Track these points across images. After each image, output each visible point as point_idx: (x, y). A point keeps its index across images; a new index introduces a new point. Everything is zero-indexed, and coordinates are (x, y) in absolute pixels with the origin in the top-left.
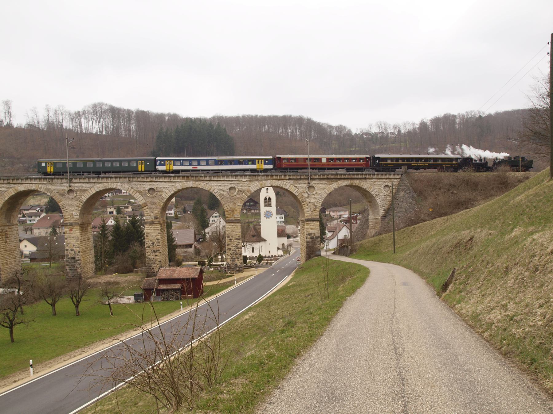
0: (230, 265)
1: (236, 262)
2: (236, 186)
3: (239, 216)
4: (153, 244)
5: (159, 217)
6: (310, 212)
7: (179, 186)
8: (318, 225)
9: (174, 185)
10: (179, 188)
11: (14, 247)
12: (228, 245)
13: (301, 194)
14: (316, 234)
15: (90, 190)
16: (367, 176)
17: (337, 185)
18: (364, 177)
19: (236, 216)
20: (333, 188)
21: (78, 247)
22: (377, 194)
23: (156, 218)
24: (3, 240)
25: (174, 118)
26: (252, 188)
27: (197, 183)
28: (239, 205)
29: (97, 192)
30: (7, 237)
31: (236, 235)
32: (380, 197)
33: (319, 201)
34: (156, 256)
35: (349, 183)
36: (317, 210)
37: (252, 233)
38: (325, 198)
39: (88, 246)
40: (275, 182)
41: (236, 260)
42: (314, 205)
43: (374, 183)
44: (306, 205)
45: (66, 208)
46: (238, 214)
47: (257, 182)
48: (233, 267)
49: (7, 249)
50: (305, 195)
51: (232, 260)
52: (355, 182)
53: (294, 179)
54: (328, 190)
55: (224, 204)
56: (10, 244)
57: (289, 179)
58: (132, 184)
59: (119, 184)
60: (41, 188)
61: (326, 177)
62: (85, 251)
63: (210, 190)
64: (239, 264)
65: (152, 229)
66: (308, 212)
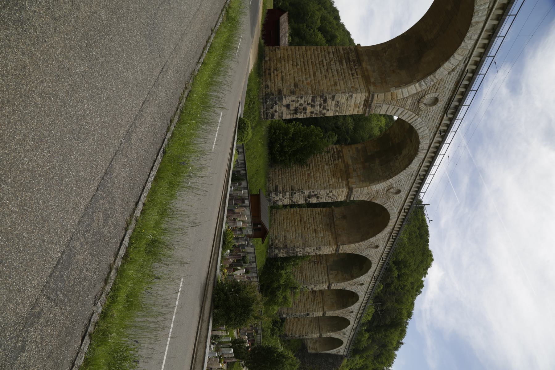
11: (305, 274)
30: (315, 264)
39: (306, 229)
56: (308, 269)
62: (301, 221)
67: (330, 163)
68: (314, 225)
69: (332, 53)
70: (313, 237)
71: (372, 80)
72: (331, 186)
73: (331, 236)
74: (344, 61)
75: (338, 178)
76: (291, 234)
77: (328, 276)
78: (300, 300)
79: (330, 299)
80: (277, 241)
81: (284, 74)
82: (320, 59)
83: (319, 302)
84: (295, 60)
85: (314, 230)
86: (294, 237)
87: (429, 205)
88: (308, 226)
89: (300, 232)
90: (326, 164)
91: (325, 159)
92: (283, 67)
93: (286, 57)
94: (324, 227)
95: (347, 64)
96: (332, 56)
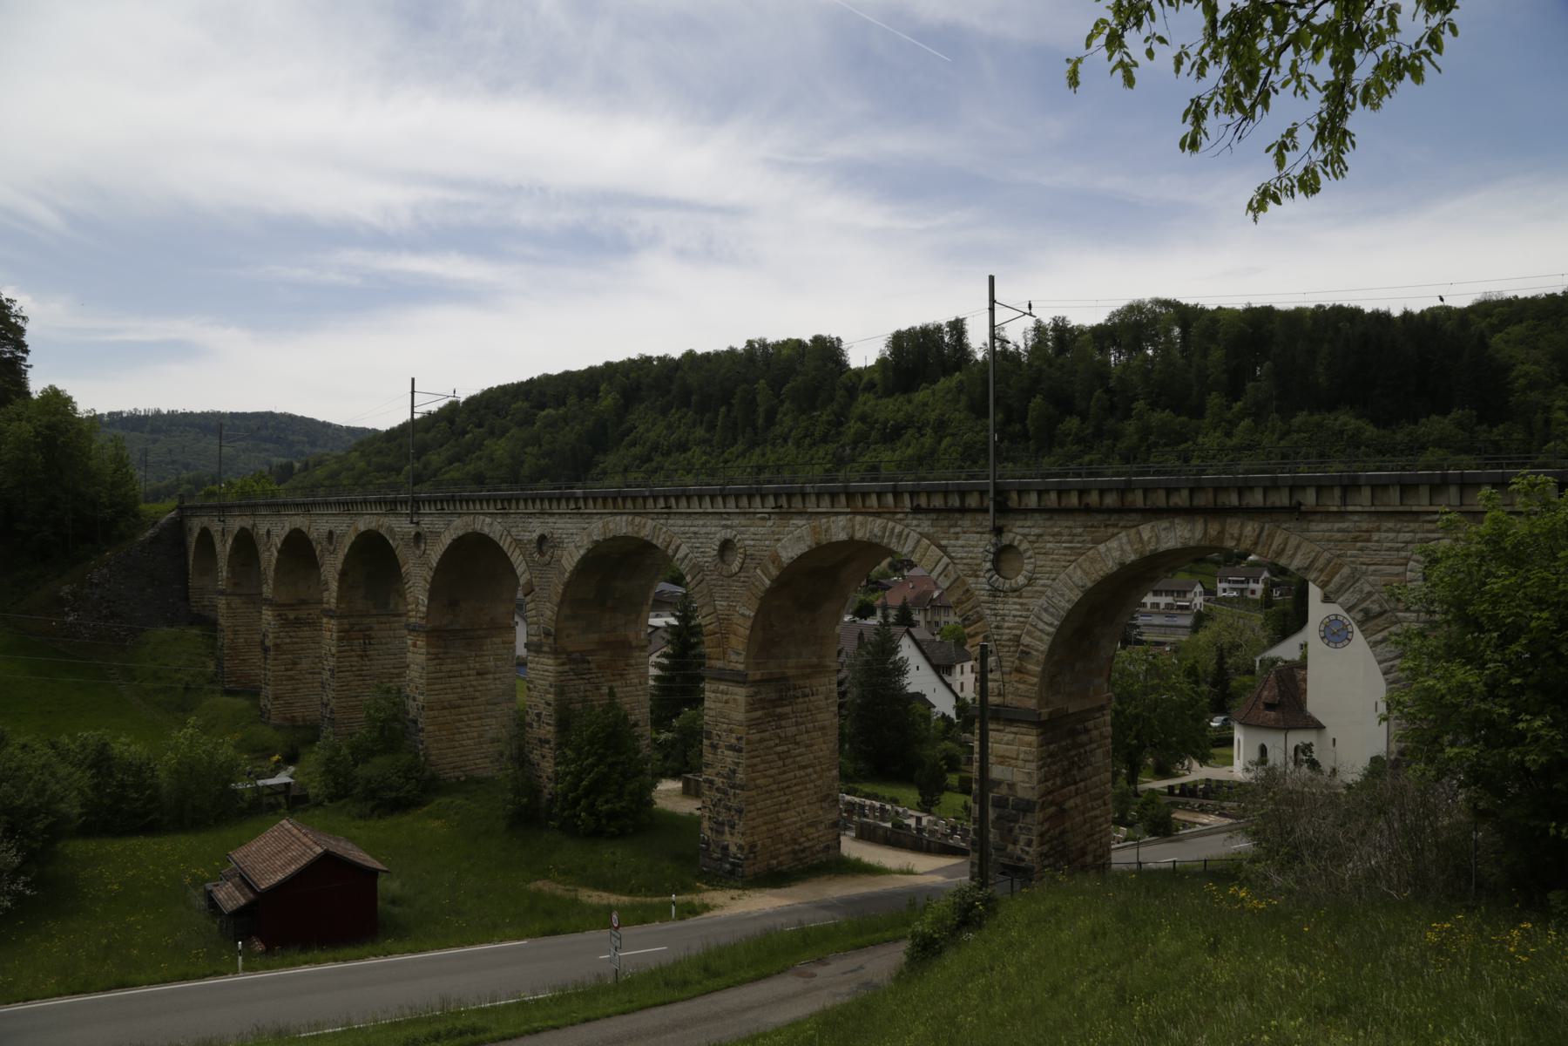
0: (708, 844)
1: (724, 838)
2: (738, 537)
3: (741, 659)
4: (539, 715)
5: (553, 630)
7: (596, 531)
8: (1030, 745)
9: (586, 526)
10: (595, 538)
11: (395, 668)
12: (707, 765)
13: (964, 583)
17: (1130, 542)
18: (1282, 499)
19: (733, 657)
20: (1110, 564)
21: (423, 694)
22: (1376, 608)
23: (548, 634)
24: (352, 650)
26: (784, 547)
27: (638, 520)
28: (743, 615)
29: (454, 540)
30: (370, 644)
31: (731, 731)
33: (1041, 625)
34: (544, 757)
35: (1198, 534)
37: (1265, 693)
38: (1071, 612)
39: (478, 694)
40: (862, 525)
41: (727, 829)
43: (1355, 540)
46: (741, 647)
47: (804, 522)
48: (715, 856)
49: (364, 673)
50: (980, 586)
51: (715, 826)
52: (1236, 532)
54: (1087, 574)
57: (917, 510)
58: (511, 519)
59: (488, 520)
60: (381, 526)
62: (459, 707)
63: (669, 545)
64: (733, 849)
65: (539, 667)
67: (597, 681)
68: (469, 675)
69: (762, 735)
70: (495, 679)
71: (815, 660)
72: (643, 680)
73: (494, 639)
74: (779, 710)
76: (487, 728)
81: (804, 824)
82: (775, 757)
84: (777, 807)
85: (479, 677)
86: (494, 721)
87: (413, 380)
88: (468, 689)
89: (482, 707)
90: (598, 688)
91: (586, 691)
92: (790, 828)
93: (771, 826)
94: (473, 654)
95: (786, 705)
96: (767, 733)
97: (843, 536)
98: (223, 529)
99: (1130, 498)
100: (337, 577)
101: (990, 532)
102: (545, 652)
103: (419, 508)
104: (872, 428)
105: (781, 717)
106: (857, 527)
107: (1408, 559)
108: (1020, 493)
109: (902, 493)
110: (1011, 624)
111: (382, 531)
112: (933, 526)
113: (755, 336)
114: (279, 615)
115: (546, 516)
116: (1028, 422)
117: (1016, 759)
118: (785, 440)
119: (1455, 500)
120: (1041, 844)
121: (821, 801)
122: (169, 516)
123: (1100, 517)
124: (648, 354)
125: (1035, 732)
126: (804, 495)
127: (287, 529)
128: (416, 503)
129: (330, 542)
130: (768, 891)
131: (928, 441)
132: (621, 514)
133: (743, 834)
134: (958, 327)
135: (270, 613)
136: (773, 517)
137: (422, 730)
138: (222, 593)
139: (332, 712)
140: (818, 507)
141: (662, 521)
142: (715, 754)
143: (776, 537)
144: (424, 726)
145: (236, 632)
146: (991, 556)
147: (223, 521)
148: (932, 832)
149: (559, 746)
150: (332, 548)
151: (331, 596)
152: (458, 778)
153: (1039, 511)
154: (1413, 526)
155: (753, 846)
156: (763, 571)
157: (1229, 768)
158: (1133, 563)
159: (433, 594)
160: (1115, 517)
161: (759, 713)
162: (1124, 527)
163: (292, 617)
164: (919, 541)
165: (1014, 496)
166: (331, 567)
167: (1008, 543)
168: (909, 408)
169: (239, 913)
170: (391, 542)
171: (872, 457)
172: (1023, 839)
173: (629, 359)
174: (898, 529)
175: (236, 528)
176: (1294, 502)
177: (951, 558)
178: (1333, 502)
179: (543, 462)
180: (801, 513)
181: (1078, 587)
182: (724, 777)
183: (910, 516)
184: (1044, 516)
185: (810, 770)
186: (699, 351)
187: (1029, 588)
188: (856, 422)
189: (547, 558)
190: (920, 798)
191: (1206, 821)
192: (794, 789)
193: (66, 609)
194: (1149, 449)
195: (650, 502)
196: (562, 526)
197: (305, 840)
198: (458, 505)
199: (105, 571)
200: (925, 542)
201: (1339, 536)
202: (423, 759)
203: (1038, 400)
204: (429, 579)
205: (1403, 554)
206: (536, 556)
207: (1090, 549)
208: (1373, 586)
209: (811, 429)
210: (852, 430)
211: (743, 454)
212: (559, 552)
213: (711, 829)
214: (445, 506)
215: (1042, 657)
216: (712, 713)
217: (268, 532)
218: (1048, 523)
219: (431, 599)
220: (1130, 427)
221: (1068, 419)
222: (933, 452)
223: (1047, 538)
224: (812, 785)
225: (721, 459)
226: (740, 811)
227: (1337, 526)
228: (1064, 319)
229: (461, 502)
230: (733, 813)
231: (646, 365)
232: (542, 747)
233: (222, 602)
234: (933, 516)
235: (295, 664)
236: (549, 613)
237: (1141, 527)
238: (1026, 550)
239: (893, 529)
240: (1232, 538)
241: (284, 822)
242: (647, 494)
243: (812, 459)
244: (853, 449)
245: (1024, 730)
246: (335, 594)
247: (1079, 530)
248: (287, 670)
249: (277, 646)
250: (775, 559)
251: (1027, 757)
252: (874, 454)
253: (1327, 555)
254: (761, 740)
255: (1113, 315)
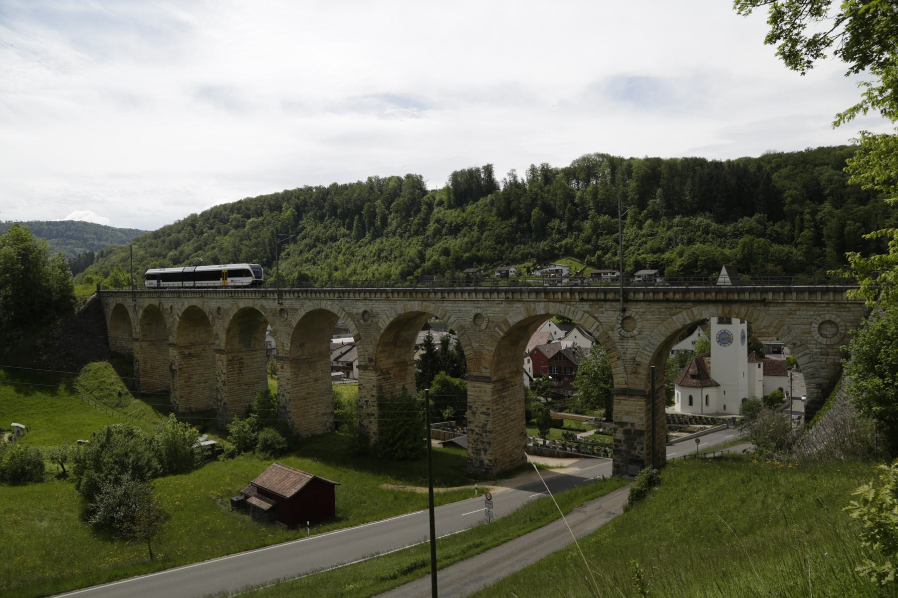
0: (472, 460)
1: (481, 457)
3: (488, 371)
4: (367, 401)
5: (374, 359)
6: (625, 375)
8: (641, 406)
10: (400, 312)
12: (470, 422)
13: (607, 334)
14: (636, 425)
15: (299, 311)
16: (770, 296)
18: (758, 296)
19: (483, 370)
21: (289, 393)
22: (799, 343)
24: (234, 371)
25: (694, 166)
26: (510, 317)
27: (425, 303)
28: (488, 350)
30: (243, 367)
31: (483, 405)
32: (807, 351)
33: (646, 352)
34: (370, 422)
36: (640, 371)
37: (691, 370)
39: (315, 391)
41: (482, 452)
42: (634, 359)
43: (789, 314)
44: (615, 359)
45: (278, 335)
48: (476, 466)
49: (240, 382)
50: (615, 335)
51: (475, 451)
53: (591, 300)
55: (465, 346)
57: (582, 300)
59: (329, 303)
61: (661, 296)
62: (305, 399)
64: (486, 462)
65: (366, 377)
66: (621, 375)
70: (323, 383)
71: (515, 369)
74: (503, 394)
75: (407, 374)
77: (256, 351)
78: (201, 376)
79: (200, 334)
80: (328, 424)
82: (502, 416)
83: (203, 350)
90: (394, 387)
93: (502, 450)
97: (543, 312)
98: (135, 305)
99: (687, 296)
100: (225, 332)
101: (619, 311)
102: (370, 370)
103: (282, 296)
104: (443, 226)
105: (504, 397)
106: (550, 308)
107: (812, 323)
108: (634, 293)
109: (574, 293)
110: (631, 352)
111: (258, 308)
112: (590, 308)
113: (372, 175)
114: (181, 352)
115: (367, 301)
116: (531, 221)
117: (635, 412)
118: (394, 234)
119: (831, 298)
120: (647, 449)
121: (520, 436)
122: (92, 297)
123: (673, 304)
124: (310, 186)
125: (644, 400)
126: (521, 292)
127: (186, 306)
128: (280, 294)
129: (219, 314)
130: (506, 481)
131: (475, 233)
132: (415, 300)
133: (491, 454)
134: (489, 170)
135: (175, 351)
136: (503, 303)
137: (290, 412)
138: (137, 340)
139: (225, 404)
140: (529, 298)
141: (439, 304)
142: (475, 416)
143: (506, 312)
144: (290, 409)
145: (145, 362)
146: (620, 322)
147: (135, 301)
148: (555, 448)
149: (381, 416)
150: (220, 317)
151: (222, 341)
152: (308, 435)
153: (644, 301)
154: (814, 309)
155: (496, 460)
156: (499, 329)
157: (672, 407)
158: (689, 325)
159: (292, 342)
160: (680, 305)
161: (496, 397)
162: (685, 308)
163: (187, 353)
164: (583, 315)
165: (632, 294)
166: (220, 328)
167: (628, 315)
168: (464, 215)
169: (270, 510)
170: (263, 313)
171: (444, 243)
172: (639, 447)
173: (298, 189)
174: (572, 309)
175: (146, 305)
176: (762, 298)
177: (600, 322)
178: (780, 297)
179: (254, 249)
180: (519, 301)
181: (663, 335)
182: (479, 427)
183: (578, 303)
184: (648, 303)
185: (515, 422)
186: (340, 183)
187: (639, 336)
188: (434, 223)
189: (369, 322)
190: (539, 432)
191: (674, 434)
192: (510, 431)
193: (41, 353)
194: (598, 238)
195: (432, 295)
196: (378, 306)
197: (297, 472)
198: (309, 294)
199: (60, 330)
200: (586, 315)
201: (782, 312)
202: (291, 427)
203: (535, 212)
204: (291, 333)
205: (809, 320)
206: (362, 322)
207: (668, 318)
208: (797, 333)
209: (409, 227)
210: (433, 228)
211: (370, 242)
212: (377, 320)
213: (474, 453)
214: (300, 294)
215: (646, 367)
216: (473, 397)
217: (171, 307)
218: (648, 307)
219: (292, 343)
220: (587, 225)
221: (553, 220)
222: (479, 240)
223: (648, 313)
224: (515, 429)
225: (357, 245)
226: (489, 443)
227: (781, 308)
228: (547, 165)
229: (311, 293)
230: (486, 444)
231: (309, 192)
232: (369, 417)
233: (136, 346)
234: (591, 303)
235: (190, 378)
236: (371, 350)
237: (693, 309)
238: (638, 319)
239: (570, 309)
240: (735, 313)
241: (274, 464)
242: (431, 291)
243: (410, 244)
244: (433, 239)
245: (638, 399)
246: (224, 342)
247: (663, 310)
248: (186, 382)
249: (180, 369)
250: (506, 322)
251: (639, 411)
252: (445, 241)
253: (777, 321)
254: (497, 409)
255: (574, 162)
